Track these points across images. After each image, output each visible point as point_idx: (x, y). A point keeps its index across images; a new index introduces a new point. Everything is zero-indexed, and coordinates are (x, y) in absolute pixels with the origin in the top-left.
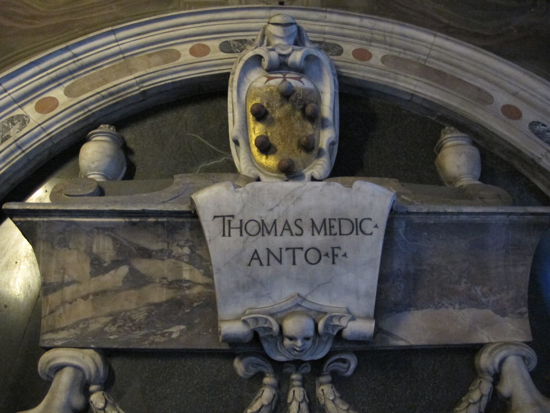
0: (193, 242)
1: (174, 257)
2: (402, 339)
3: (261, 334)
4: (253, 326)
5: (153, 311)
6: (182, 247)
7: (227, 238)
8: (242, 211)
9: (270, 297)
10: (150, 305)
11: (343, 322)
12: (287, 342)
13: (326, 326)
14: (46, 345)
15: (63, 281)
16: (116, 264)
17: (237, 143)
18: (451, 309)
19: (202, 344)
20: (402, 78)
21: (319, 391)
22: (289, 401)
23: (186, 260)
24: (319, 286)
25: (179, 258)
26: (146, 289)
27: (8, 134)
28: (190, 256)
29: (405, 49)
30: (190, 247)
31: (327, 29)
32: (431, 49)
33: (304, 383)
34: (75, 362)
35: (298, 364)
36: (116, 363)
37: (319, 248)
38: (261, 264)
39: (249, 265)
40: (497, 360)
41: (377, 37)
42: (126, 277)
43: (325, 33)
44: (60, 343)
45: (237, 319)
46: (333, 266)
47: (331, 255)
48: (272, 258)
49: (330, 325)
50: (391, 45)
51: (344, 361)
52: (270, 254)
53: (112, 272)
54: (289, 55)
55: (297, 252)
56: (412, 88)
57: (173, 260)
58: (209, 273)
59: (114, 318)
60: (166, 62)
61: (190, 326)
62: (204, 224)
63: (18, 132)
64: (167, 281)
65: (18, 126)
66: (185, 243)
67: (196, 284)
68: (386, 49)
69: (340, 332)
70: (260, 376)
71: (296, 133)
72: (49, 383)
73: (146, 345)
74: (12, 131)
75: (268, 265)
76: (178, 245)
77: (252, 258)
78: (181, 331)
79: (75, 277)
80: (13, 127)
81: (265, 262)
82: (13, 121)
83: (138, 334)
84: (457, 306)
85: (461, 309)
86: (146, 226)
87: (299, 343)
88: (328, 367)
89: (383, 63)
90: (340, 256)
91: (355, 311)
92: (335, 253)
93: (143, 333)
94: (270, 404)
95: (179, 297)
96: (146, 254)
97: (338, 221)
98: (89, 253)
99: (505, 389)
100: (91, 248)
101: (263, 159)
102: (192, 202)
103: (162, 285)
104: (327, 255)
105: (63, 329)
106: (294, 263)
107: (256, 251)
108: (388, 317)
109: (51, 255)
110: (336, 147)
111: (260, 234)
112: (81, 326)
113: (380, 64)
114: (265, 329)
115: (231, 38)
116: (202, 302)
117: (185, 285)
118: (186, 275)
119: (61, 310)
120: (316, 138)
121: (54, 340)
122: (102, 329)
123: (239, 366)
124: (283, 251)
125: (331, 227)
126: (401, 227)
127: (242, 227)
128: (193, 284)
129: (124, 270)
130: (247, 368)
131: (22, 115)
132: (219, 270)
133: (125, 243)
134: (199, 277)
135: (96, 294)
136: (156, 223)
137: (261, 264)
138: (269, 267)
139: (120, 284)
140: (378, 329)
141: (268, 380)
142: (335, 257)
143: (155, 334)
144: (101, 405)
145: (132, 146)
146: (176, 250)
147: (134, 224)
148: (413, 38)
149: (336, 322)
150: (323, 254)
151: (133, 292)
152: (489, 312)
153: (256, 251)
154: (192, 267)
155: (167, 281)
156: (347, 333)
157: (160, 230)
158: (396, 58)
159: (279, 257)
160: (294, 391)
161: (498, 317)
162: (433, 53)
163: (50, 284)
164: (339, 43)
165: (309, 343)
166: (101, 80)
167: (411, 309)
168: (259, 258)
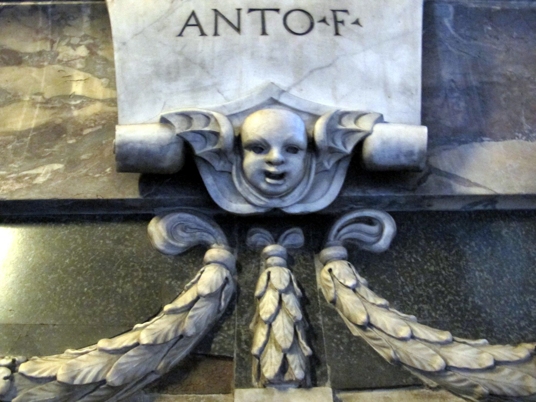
0: (94, 39)
1: (60, 61)
3: (199, 149)
4: (180, 127)
5: (9, 143)
6: (75, 47)
9: (219, 91)
21: (323, 275)
22: (257, 293)
23: (79, 66)
24: (311, 72)
25: (69, 63)
28: (86, 60)
30: (88, 47)
37: (308, 10)
38: (203, 34)
39: (180, 35)
46: (337, 38)
47: (331, 22)
48: (222, 24)
49: (338, 130)
51: (370, 221)
55: (268, 15)
57: (58, 67)
64: (44, 98)
66: (81, 41)
67: (91, 100)
69: (360, 146)
75: (216, 34)
76: (68, 44)
77: (187, 25)
78: (55, 173)
81: (209, 29)
87: (275, 154)
90: (348, 23)
95: (59, 121)
104: (324, 20)
106: (264, 33)
107: (193, 14)
108: (445, 150)
116: (100, 127)
117: (73, 103)
118: (77, 89)
124: (244, 14)
130: (171, 232)
132: (124, 44)
137: (203, 34)
138: (216, 38)
142: (340, 25)
149: (349, 125)
150: (316, 20)
153: (193, 14)
154: (88, 75)
155: (44, 98)
159: (236, 24)
160: (269, 274)
167: (484, 139)
168: (198, 25)
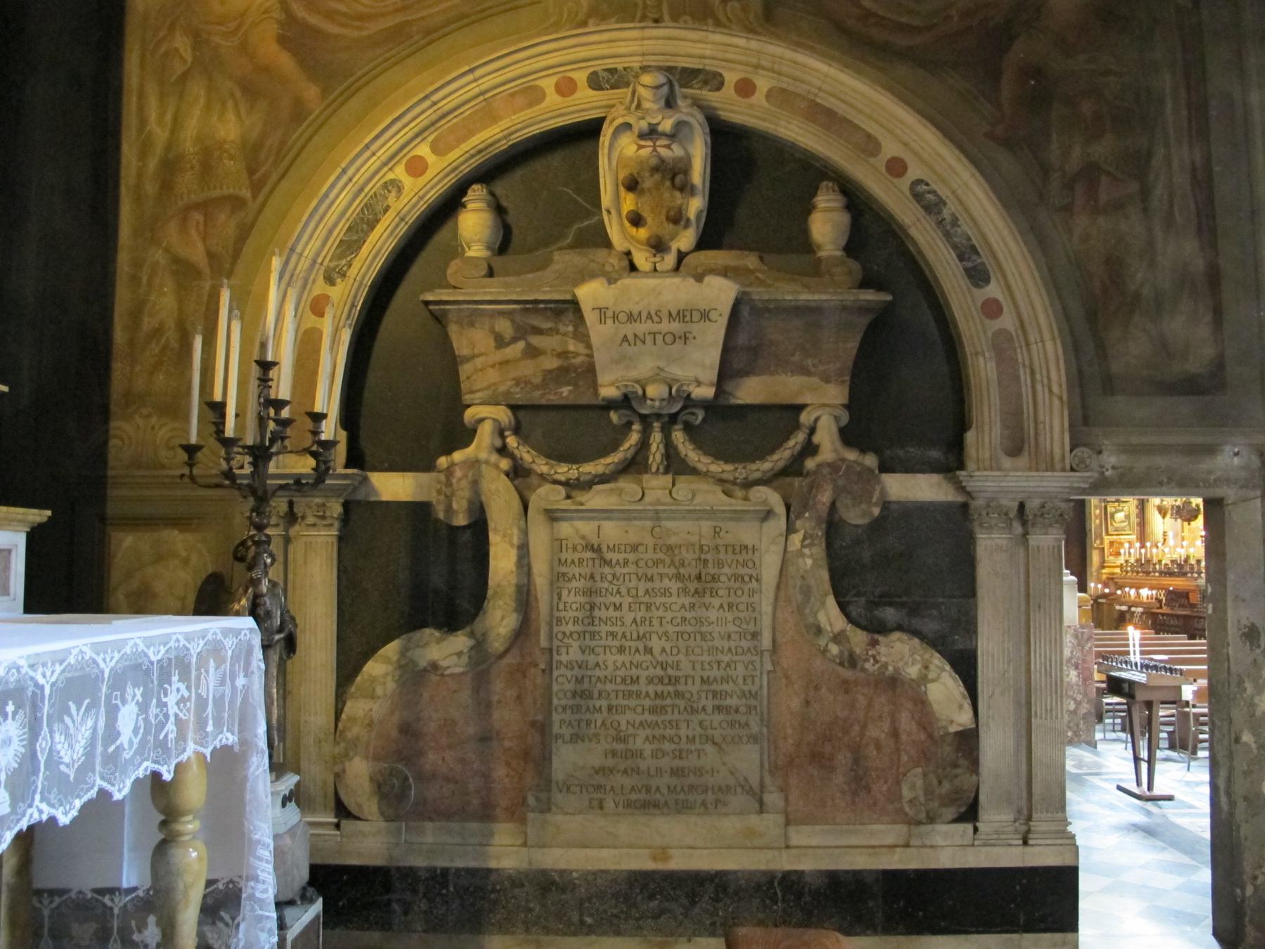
3: (630, 396)
4: (623, 390)
6: (567, 326)
7: (603, 326)
10: (544, 371)
11: (691, 388)
12: (649, 402)
13: (678, 390)
14: (468, 402)
16: (515, 340)
17: (609, 212)
19: (585, 400)
20: (783, 123)
21: (673, 435)
25: (565, 334)
26: (542, 358)
29: (794, 79)
31: (708, 53)
32: (823, 82)
33: (663, 429)
34: (494, 416)
35: (658, 416)
36: (521, 414)
40: (813, 418)
41: (764, 63)
42: (523, 350)
43: (704, 57)
44: (478, 401)
45: (612, 384)
50: (780, 74)
51: (693, 414)
53: (512, 346)
54: (659, 124)
55: (657, 336)
56: (794, 135)
58: (589, 346)
59: (518, 382)
60: (530, 105)
61: (576, 385)
65: (393, 194)
68: (773, 78)
69: (689, 395)
72: (475, 431)
73: (543, 402)
79: (483, 350)
81: (632, 343)
84: (789, 374)
85: (792, 376)
86: (537, 311)
87: (657, 403)
88: (682, 417)
89: (767, 101)
91: (702, 378)
93: (540, 392)
94: (637, 444)
96: (538, 331)
98: (492, 331)
99: (816, 439)
101: (633, 230)
102: (574, 295)
103: (553, 356)
107: (625, 336)
115: (598, 66)
118: (571, 348)
119: (474, 377)
120: (684, 207)
121: (473, 399)
123: (614, 416)
125: (684, 316)
126: (745, 311)
128: (577, 354)
129: (521, 345)
130: (619, 418)
131: (395, 180)
134: (581, 349)
135: (501, 363)
136: (545, 309)
139: (519, 355)
140: (717, 395)
141: (636, 427)
143: (549, 393)
144: (515, 445)
145: (505, 203)
146: (562, 328)
147: (527, 310)
148: (805, 66)
149: (685, 388)
151: (529, 361)
152: (815, 380)
153: (625, 336)
156: (693, 396)
157: (549, 313)
158: (783, 91)
161: (823, 383)
162: (825, 87)
164: (720, 71)
165: (665, 403)
168: (628, 341)
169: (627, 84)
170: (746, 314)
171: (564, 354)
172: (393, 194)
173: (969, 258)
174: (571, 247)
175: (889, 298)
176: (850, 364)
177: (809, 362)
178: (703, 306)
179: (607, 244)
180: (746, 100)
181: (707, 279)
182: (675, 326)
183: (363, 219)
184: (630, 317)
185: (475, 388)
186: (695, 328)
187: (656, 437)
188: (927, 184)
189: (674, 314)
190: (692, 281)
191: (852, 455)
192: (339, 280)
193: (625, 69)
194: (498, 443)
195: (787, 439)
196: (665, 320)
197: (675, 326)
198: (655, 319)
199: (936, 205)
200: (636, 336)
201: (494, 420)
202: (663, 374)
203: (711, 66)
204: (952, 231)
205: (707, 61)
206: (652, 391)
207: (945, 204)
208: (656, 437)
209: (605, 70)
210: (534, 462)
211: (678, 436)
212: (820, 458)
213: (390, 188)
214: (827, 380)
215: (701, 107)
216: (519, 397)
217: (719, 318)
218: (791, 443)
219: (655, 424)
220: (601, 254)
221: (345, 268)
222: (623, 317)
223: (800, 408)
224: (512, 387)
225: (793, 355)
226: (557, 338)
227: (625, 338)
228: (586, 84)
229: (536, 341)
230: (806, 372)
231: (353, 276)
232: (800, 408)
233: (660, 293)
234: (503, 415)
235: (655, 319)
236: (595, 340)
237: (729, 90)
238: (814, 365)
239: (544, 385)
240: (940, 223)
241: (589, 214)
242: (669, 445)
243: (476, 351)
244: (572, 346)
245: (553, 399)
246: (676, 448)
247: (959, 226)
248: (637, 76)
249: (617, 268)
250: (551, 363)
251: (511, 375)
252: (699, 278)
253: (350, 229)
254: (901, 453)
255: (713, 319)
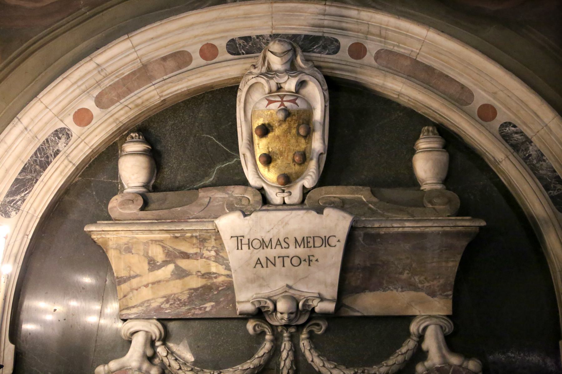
0: (217, 248)
1: (205, 257)
2: (358, 312)
5: (192, 293)
7: (240, 251)
8: (249, 233)
9: (269, 287)
10: (190, 289)
12: (279, 315)
13: (304, 305)
15: (130, 275)
16: (165, 263)
18: (395, 291)
22: (282, 350)
23: (213, 259)
24: (300, 280)
25: (208, 258)
26: (187, 279)
27: (57, 148)
28: (215, 257)
30: (215, 251)
31: (326, 23)
37: (300, 256)
38: (262, 267)
39: (255, 267)
43: (324, 27)
44: (133, 316)
46: (310, 267)
47: (307, 261)
49: (306, 305)
52: (268, 261)
53: (163, 268)
55: (285, 259)
57: (204, 260)
58: (228, 268)
61: (218, 303)
62: (225, 242)
63: (65, 146)
64: (201, 273)
65: (63, 140)
66: (212, 248)
67: (220, 275)
68: (381, 42)
69: (314, 308)
70: (263, 333)
71: (292, 148)
72: (130, 342)
73: (189, 316)
74: (59, 144)
75: (267, 267)
76: (207, 250)
77: (257, 263)
78: (212, 306)
79: (138, 272)
80: (60, 141)
81: (264, 265)
82: (58, 135)
83: (184, 309)
84: (400, 289)
85: (402, 291)
86: (184, 239)
89: (376, 61)
90: (314, 261)
92: (311, 259)
93: (187, 308)
94: (269, 352)
95: (209, 284)
96: (186, 256)
97: (312, 238)
98: (146, 255)
99: (424, 346)
100: (148, 253)
103: (198, 276)
105: (133, 307)
106: (284, 266)
107: (259, 259)
108: (350, 296)
109: (120, 258)
110: (325, 156)
111: (262, 248)
112: (146, 305)
113: (374, 63)
114: (264, 307)
116: (225, 287)
117: (213, 276)
118: (213, 270)
119: (131, 295)
120: (308, 150)
121: (129, 314)
122: (160, 306)
124: (277, 258)
125: (308, 242)
127: (250, 244)
128: (217, 275)
129: (171, 267)
131: (65, 128)
132: (236, 271)
133: (171, 249)
134: (221, 270)
135: (153, 283)
136: (192, 237)
137: (262, 267)
138: (267, 268)
139: (170, 276)
140: (337, 308)
142: (311, 262)
143: (194, 308)
147: (177, 237)
149: (310, 303)
150: (302, 260)
151: (178, 281)
152: (423, 294)
153: (259, 259)
154: (217, 264)
155: (201, 273)
156: (317, 310)
157: (195, 241)
159: (274, 262)
160: (285, 344)
161: (430, 298)
163: (121, 277)
164: (336, 37)
166: (124, 89)
167: (366, 291)
168: (261, 263)
169: (260, 50)
170: (361, 239)
171: (207, 275)
172: (63, 140)
173: (555, 187)
174: (213, 185)
175: (483, 223)
176: (452, 280)
177: (417, 279)
178: (324, 233)
179: (245, 183)
180: (358, 61)
181: (326, 211)
182: (301, 251)
183: (36, 161)
184: (263, 244)
185: (130, 305)
186: (318, 252)
187: (286, 346)
188: (515, 126)
189: (299, 240)
190: (314, 213)
191: (455, 360)
192: (13, 213)
193: (258, 37)
194: (149, 353)
195: (400, 346)
196: (292, 247)
197: (301, 251)
198: (284, 245)
199: (523, 143)
200: (267, 258)
201: (147, 332)
202: (292, 292)
203: (328, 33)
204: (538, 165)
205: (325, 30)
206: (282, 306)
207: (531, 142)
208: (286, 346)
209: (241, 38)
210: (180, 369)
211: (304, 344)
212: (427, 364)
213: (60, 135)
214: (433, 294)
215: (319, 67)
216: (168, 312)
217: (338, 244)
218: (404, 350)
219: (285, 334)
220: (237, 191)
221: (19, 203)
222: (256, 244)
223: (410, 319)
224: (162, 304)
225: (401, 273)
226: (202, 261)
227: (259, 261)
228: (225, 50)
229: (184, 264)
230: (413, 287)
231: (26, 210)
232: (410, 319)
233: (287, 224)
234: (155, 329)
235: (284, 245)
236: (233, 263)
237: (343, 54)
238: (420, 282)
239: (191, 300)
240: (526, 159)
241: (229, 157)
242: (296, 351)
243: (132, 273)
244: (214, 268)
245: (198, 313)
246: (304, 355)
247: (544, 161)
248: (267, 43)
249: (251, 202)
250: (196, 283)
251: (163, 293)
252: (320, 211)
253: (24, 169)
254: (502, 357)
255: (333, 244)
